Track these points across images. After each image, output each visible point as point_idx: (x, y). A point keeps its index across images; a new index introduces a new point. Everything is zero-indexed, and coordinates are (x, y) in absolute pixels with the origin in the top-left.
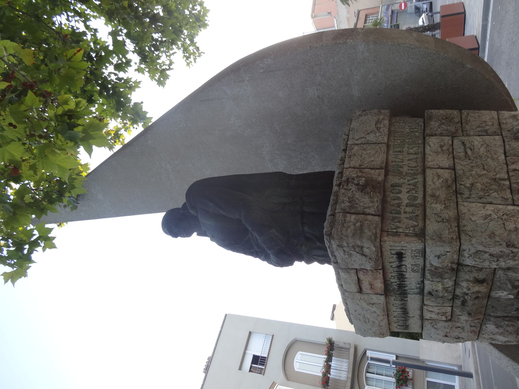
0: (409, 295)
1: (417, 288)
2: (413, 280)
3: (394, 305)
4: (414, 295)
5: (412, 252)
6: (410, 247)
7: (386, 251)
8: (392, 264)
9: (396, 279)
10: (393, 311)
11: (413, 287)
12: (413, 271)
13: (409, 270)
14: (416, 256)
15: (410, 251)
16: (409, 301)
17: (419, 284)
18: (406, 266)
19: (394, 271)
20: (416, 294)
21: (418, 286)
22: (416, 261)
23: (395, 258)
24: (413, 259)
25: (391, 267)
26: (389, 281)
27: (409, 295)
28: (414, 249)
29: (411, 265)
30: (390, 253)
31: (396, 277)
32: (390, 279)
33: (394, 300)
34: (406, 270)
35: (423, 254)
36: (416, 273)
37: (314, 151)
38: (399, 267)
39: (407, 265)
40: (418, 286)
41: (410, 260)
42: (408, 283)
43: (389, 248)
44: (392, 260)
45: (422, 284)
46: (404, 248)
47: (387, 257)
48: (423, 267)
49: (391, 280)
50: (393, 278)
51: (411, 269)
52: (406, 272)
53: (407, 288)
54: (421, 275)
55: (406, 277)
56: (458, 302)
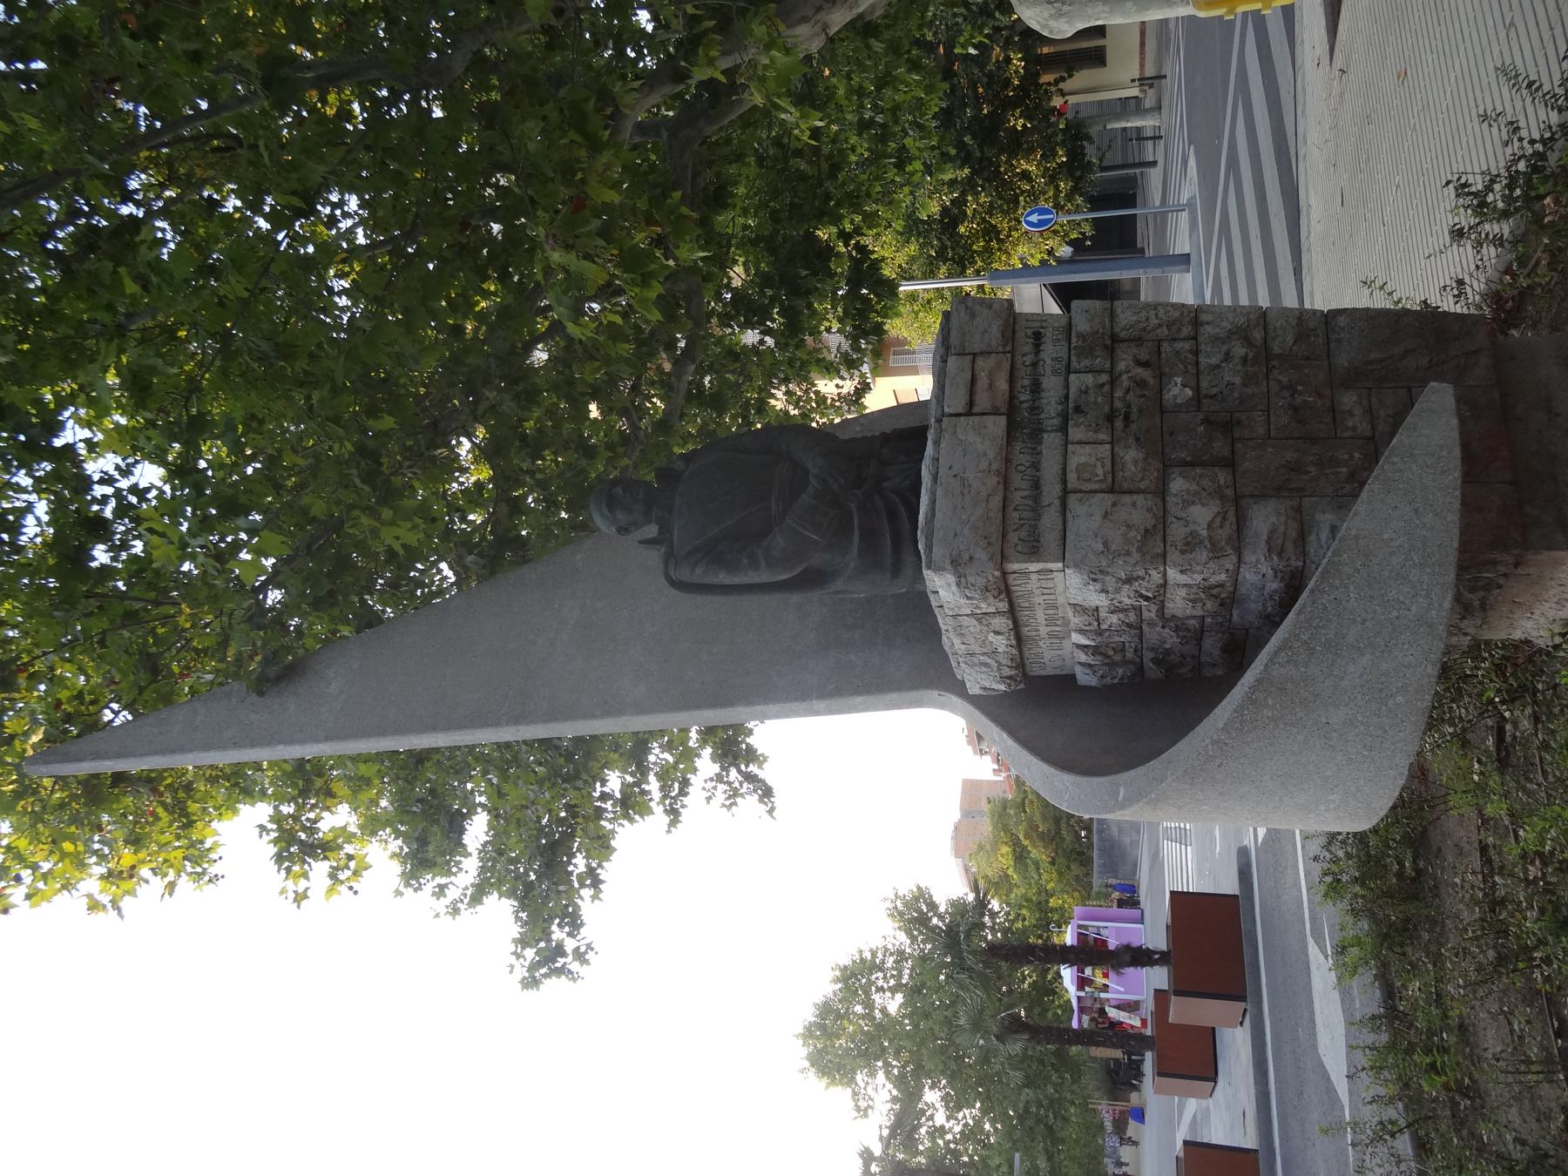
0: (1046, 436)
1: (1058, 415)
12: (1055, 372)
13: (1048, 370)
20: (1056, 431)
27: (1046, 436)
38: (1034, 365)
40: (1060, 408)
53: (1043, 416)
56: (1119, 424)
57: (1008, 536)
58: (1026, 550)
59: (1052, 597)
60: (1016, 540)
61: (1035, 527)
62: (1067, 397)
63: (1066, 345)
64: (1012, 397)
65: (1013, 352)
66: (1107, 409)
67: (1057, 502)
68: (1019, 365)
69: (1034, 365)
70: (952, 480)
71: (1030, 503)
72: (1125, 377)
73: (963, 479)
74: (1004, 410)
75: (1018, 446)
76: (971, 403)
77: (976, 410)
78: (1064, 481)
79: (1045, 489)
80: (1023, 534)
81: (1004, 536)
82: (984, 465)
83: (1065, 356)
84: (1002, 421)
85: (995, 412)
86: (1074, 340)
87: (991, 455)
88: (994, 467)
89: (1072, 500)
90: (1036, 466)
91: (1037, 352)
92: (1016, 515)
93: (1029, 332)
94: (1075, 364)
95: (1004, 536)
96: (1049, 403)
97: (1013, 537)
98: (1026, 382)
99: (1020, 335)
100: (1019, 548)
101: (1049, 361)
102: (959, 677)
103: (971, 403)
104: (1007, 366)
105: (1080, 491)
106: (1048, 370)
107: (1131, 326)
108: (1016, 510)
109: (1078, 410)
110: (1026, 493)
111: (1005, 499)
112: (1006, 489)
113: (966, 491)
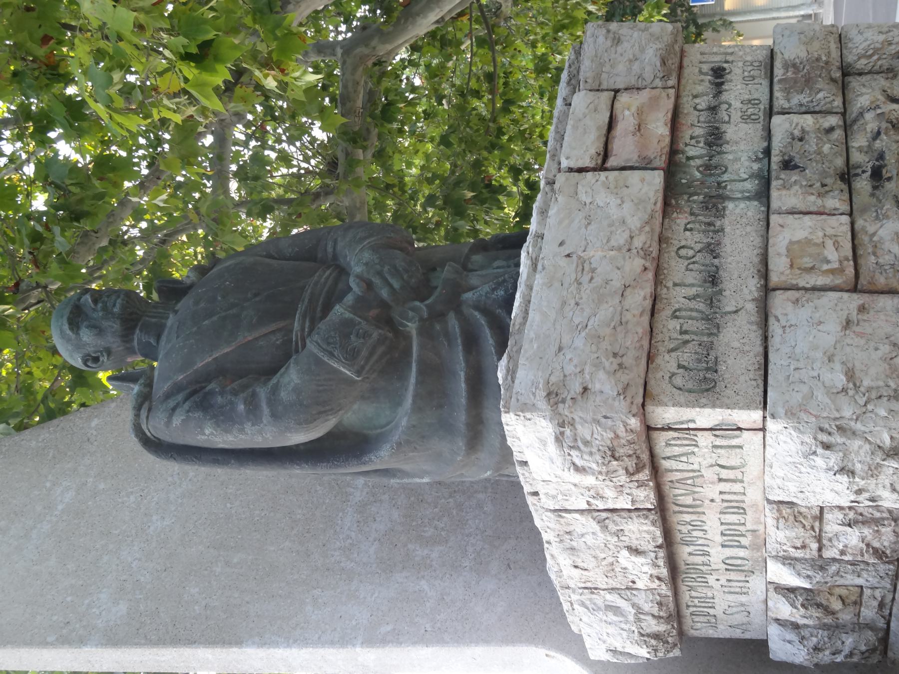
0: (730, 205)
1: (752, 176)
3: (683, 252)
4: (742, 205)
5: (745, 68)
6: (741, 53)
7: (690, 66)
8: (697, 101)
9: (702, 145)
10: (675, 285)
11: (742, 170)
12: (746, 118)
13: (736, 116)
14: (754, 78)
15: (740, 64)
16: (728, 229)
17: (758, 160)
18: (730, 105)
19: (699, 122)
20: (748, 198)
21: (756, 166)
22: (753, 91)
23: (707, 84)
24: (747, 85)
25: (695, 108)
26: (683, 152)
27: (730, 205)
28: (749, 58)
29: (742, 103)
30: (697, 70)
31: (702, 139)
32: (686, 145)
33: (686, 229)
34: (730, 116)
35: (769, 71)
36: (751, 125)
37: (490, 490)
38: (713, 109)
39: (733, 103)
40: (756, 166)
41: (739, 87)
42: (730, 157)
43: (699, 56)
44: (700, 89)
45: (766, 160)
46: (730, 58)
47: (690, 81)
48: (767, 106)
49: (687, 149)
50: (693, 142)
51: (740, 114)
52: (729, 122)
53: (725, 177)
54: (763, 130)
55: (728, 139)
56: (863, 184)
57: (659, 360)
58: (690, 385)
59: (737, 487)
60: (673, 368)
61: (710, 347)
62: (767, 152)
63: (765, 83)
64: (673, 151)
65: (678, 88)
66: (840, 162)
67: (751, 307)
68: (687, 104)
69: (713, 109)
70: (563, 262)
71: (702, 306)
72: (869, 116)
73: (582, 262)
74: (661, 162)
75: (681, 219)
76: (606, 154)
77: (611, 162)
78: (765, 274)
79: (729, 285)
80: (686, 356)
81: (650, 358)
82: (621, 238)
83: (765, 98)
84: (657, 179)
85: (645, 165)
86: (779, 72)
87: (635, 222)
88: (638, 243)
89: (780, 303)
90: (713, 250)
91: (718, 93)
92: (674, 324)
93: (706, 68)
94: (780, 101)
95: (650, 358)
96: (737, 160)
97: (667, 362)
98: (698, 131)
99: (691, 72)
100: (678, 381)
101: (736, 104)
102: (574, 628)
103: (606, 154)
104: (669, 104)
105: (797, 288)
106: (736, 116)
107: (876, 51)
108: (675, 316)
109: (788, 165)
110: (693, 291)
111: (655, 299)
112: (658, 281)
113: (585, 279)
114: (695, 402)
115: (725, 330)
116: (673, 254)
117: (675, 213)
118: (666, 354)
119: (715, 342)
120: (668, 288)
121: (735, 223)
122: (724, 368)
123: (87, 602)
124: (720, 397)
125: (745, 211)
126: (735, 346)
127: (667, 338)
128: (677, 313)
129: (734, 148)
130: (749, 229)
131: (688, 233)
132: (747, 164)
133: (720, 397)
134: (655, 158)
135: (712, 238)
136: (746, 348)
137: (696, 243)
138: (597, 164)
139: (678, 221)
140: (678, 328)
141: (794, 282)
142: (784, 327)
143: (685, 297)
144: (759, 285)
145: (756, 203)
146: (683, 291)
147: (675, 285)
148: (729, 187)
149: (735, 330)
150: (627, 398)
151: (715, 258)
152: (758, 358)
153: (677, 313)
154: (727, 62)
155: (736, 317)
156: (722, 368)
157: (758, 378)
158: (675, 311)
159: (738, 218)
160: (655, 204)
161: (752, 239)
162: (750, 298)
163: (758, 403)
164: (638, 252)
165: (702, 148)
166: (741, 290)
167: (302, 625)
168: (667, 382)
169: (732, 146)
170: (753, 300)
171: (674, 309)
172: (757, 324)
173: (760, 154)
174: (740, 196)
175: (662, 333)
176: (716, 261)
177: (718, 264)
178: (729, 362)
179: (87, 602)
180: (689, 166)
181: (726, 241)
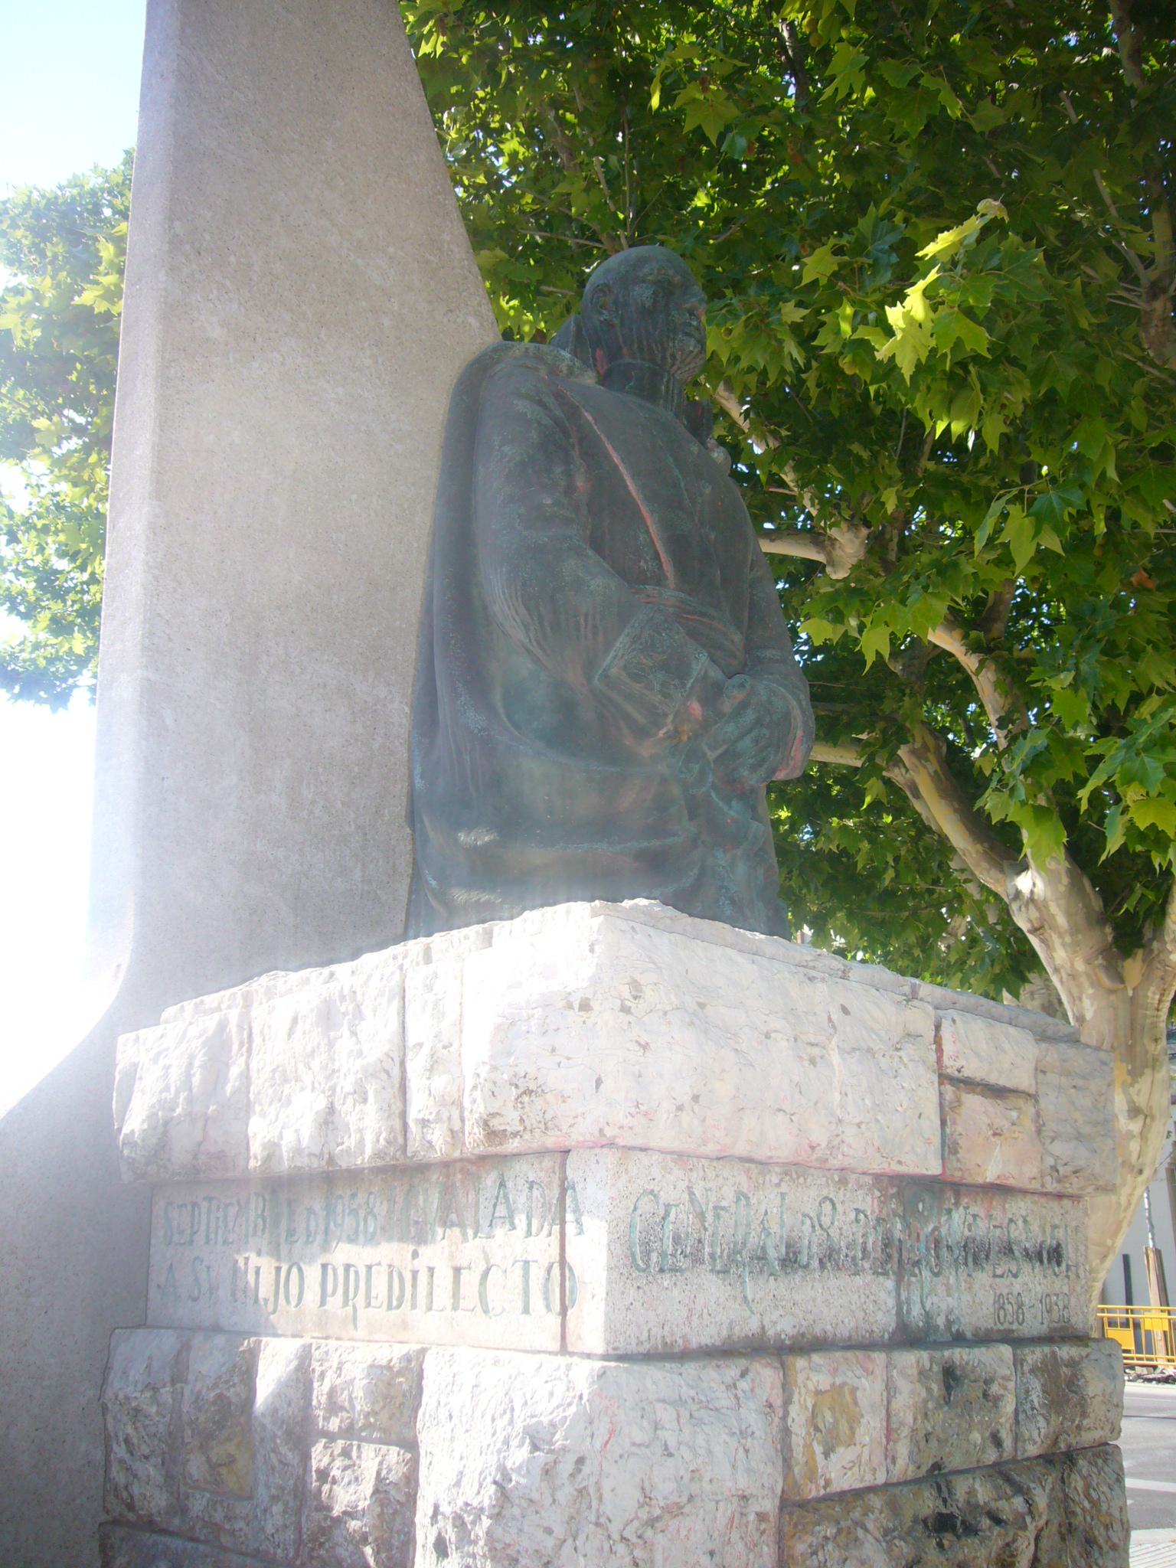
0: (890, 1284)
1: (928, 1316)
2: (966, 1298)
3: (827, 1206)
4: (891, 1302)
5: (1061, 1297)
6: (1078, 1289)
8: (1020, 1223)
11: (935, 1300)
12: (1000, 1303)
15: (1065, 1289)
16: (859, 1281)
17: (949, 1323)
18: (1015, 1276)
19: (995, 1227)
20: (899, 1313)
21: (940, 1321)
22: (1033, 1310)
24: (1041, 1302)
25: (1011, 1220)
26: (957, 1204)
28: (1073, 1301)
29: (1019, 1294)
30: (1057, 1221)
33: (858, 1211)
34: (1001, 1276)
36: (992, 1310)
37: (366, 888)
38: (1008, 1250)
39: (1019, 1280)
40: (940, 1321)
41: (1039, 1289)
42: (952, 1280)
44: (1035, 1227)
50: (970, 1219)
51: (1005, 1291)
52: (995, 1276)
54: (987, 1329)
59: (443, 1295)
66: (955, 1462)
72: (1018, 1502)
85: (949, 1148)
86: (1065, 1352)
89: (766, 1375)
90: (829, 1258)
93: (1060, 1234)
98: (982, 1229)
102: (171, 1011)
105: (787, 1402)
107: (1095, 1504)
109: (950, 1376)
114: (616, 1236)
115: (720, 1282)
116: (825, 1192)
117: (879, 1194)
118: (686, 1183)
119: (704, 1267)
120: (778, 1185)
121: (867, 1292)
122: (665, 1284)
123: (228, 283)
124: (624, 1278)
125: (883, 1307)
126: (697, 1301)
127: (709, 1185)
128: (743, 1202)
129: (963, 1284)
130: (860, 1315)
131: (853, 1215)
132: (944, 1306)
133: (624, 1278)
134: (958, 1160)
135: (847, 1256)
136: (695, 1320)
137: (840, 1229)
138: (947, 1067)
139: (869, 1199)
140: (724, 1204)
141: (795, 1398)
142: (735, 1386)
143: (766, 1213)
144: (783, 1336)
145: (893, 1325)
146: (775, 1210)
147: (783, 1195)
148: (913, 1279)
149: (721, 1300)
150: (630, 1118)
151: (821, 1261)
152: (680, 1342)
153: (743, 1202)
154: (1068, 1267)
155: (739, 1300)
156: (666, 1280)
157: (653, 1341)
158: (747, 1198)
159: (873, 1297)
160: (900, 1162)
161: (846, 1320)
162: (765, 1323)
163: (616, 1345)
164: (837, 1135)
165: (962, 1233)
166: (776, 1307)
167: (180, 590)
168: (647, 1186)
169: (965, 1281)
170: (763, 1328)
171: (750, 1195)
172: (729, 1337)
173: (957, 1327)
174: (903, 1298)
175: (717, 1176)
176: (815, 1263)
177: (811, 1267)
178: (676, 1292)
179: (228, 283)
180: (939, 1214)
181: (844, 1280)
